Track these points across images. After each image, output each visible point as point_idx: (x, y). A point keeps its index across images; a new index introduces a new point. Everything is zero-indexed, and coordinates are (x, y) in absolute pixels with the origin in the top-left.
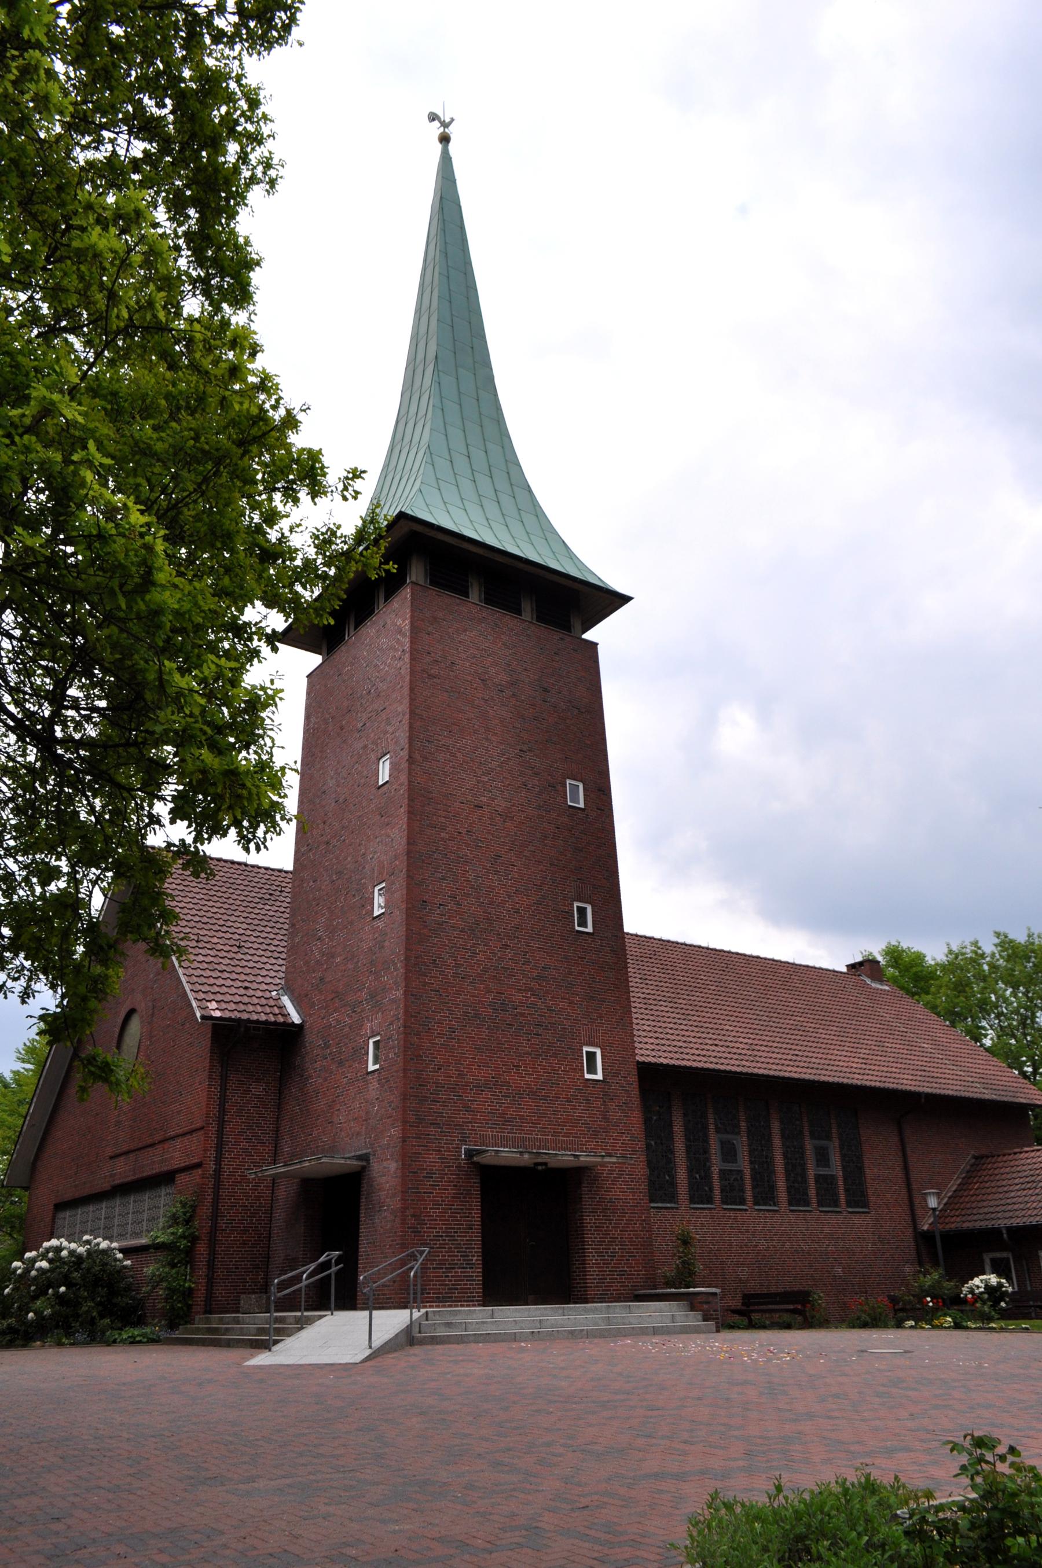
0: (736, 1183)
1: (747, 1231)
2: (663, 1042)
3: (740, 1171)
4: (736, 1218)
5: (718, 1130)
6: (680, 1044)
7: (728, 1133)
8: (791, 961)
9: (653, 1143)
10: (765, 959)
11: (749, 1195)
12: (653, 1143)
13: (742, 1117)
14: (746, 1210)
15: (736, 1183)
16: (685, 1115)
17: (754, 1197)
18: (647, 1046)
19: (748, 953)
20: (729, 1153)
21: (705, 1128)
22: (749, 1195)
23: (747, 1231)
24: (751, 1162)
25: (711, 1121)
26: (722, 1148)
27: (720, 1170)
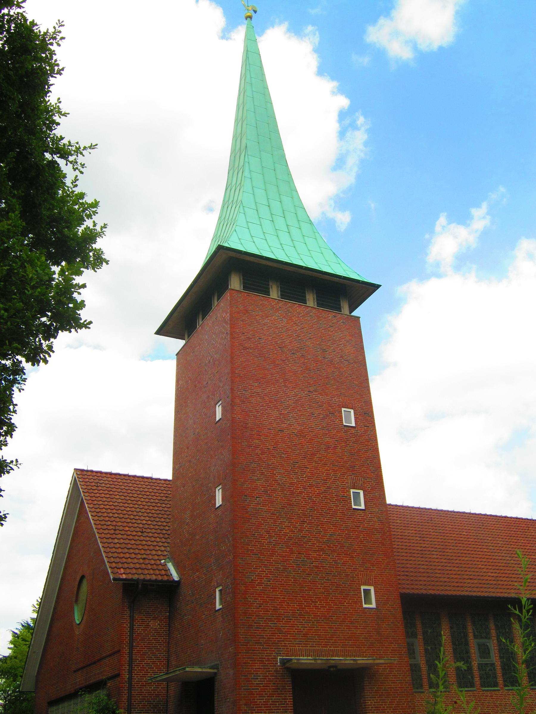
0: (490, 672)
1: (501, 705)
2: (432, 579)
3: (494, 664)
4: (491, 696)
5: (475, 637)
6: (445, 579)
7: (482, 638)
8: (530, 518)
9: (429, 648)
10: (511, 518)
11: (500, 680)
12: (429, 648)
13: (492, 626)
14: (499, 690)
15: (490, 672)
16: (451, 628)
17: (504, 681)
18: (421, 583)
19: (499, 514)
20: (484, 652)
21: (466, 636)
22: (500, 680)
23: (501, 705)
24: (501, 658)
25: (470, 631)
26: (479, 649)
27: (479, 664)
